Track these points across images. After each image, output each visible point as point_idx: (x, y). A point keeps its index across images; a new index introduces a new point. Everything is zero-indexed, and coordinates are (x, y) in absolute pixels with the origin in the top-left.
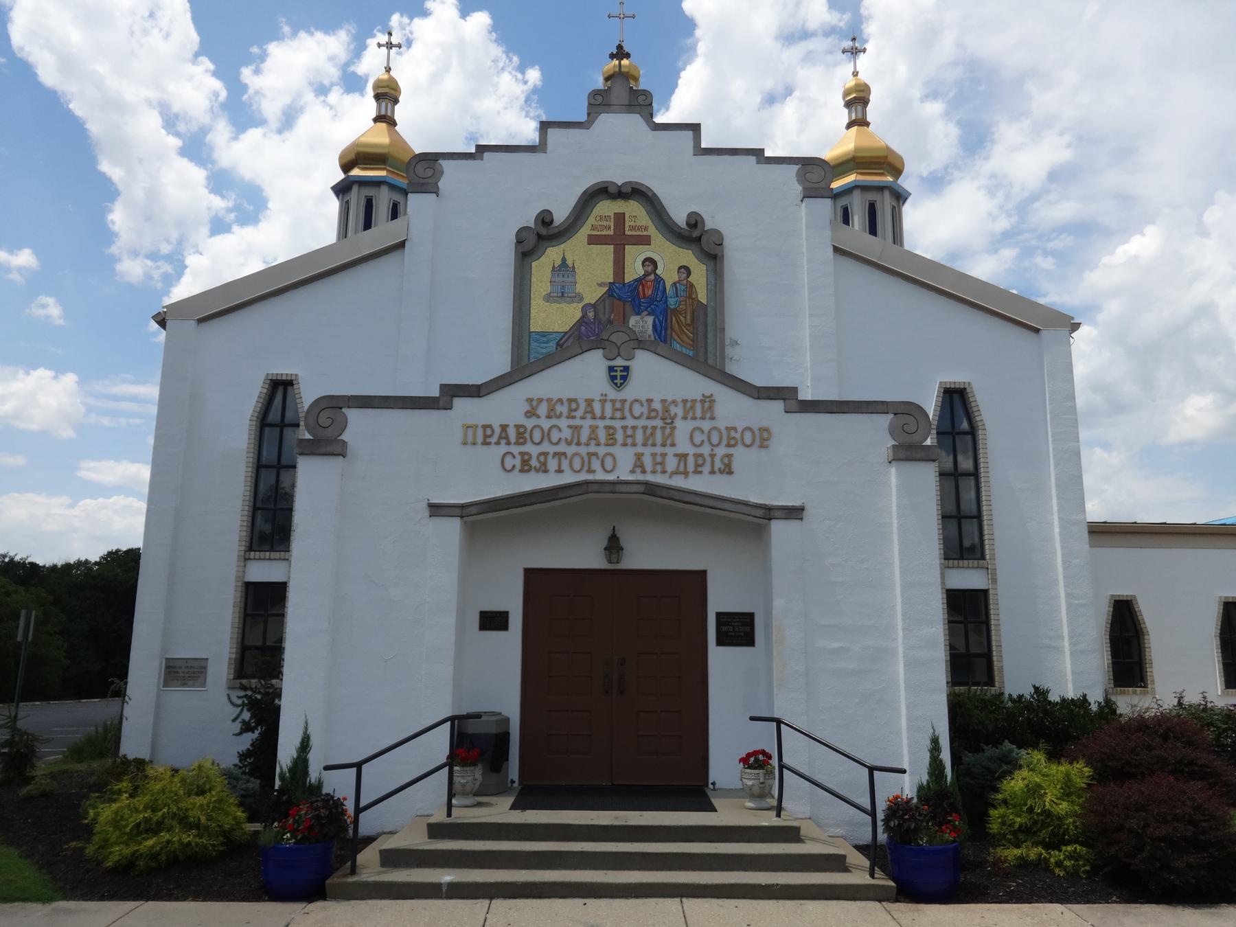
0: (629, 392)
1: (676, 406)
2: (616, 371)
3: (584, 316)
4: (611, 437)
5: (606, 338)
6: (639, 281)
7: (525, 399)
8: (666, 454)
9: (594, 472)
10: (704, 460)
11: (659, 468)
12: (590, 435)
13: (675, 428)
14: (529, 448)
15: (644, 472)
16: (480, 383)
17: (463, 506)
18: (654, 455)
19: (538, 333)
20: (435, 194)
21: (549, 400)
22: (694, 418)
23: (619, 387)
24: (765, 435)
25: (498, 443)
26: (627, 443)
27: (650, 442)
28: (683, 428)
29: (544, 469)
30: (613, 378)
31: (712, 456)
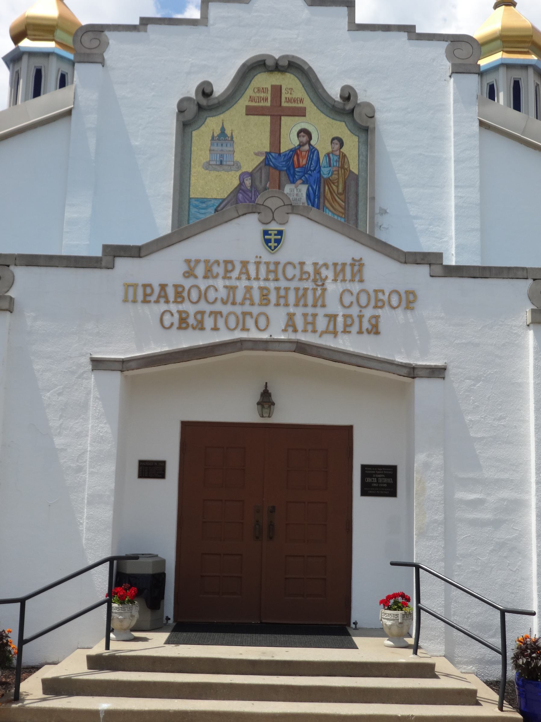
2: (271, 235)
3: (242, 183)
6: (295, 151)
7: (184, 260)
14: (186, 306)
15: (295, 331)
16: (139, 243)
17: (123, 361)
18: (305, 315)
19: (197, 199)
20: (100, 66)
21: (207, 262)
22: (344, 280)
23: (273, 250)
25: (157, 302)
27: (302, 303)
30: (267, 241)
31: (361, 317)
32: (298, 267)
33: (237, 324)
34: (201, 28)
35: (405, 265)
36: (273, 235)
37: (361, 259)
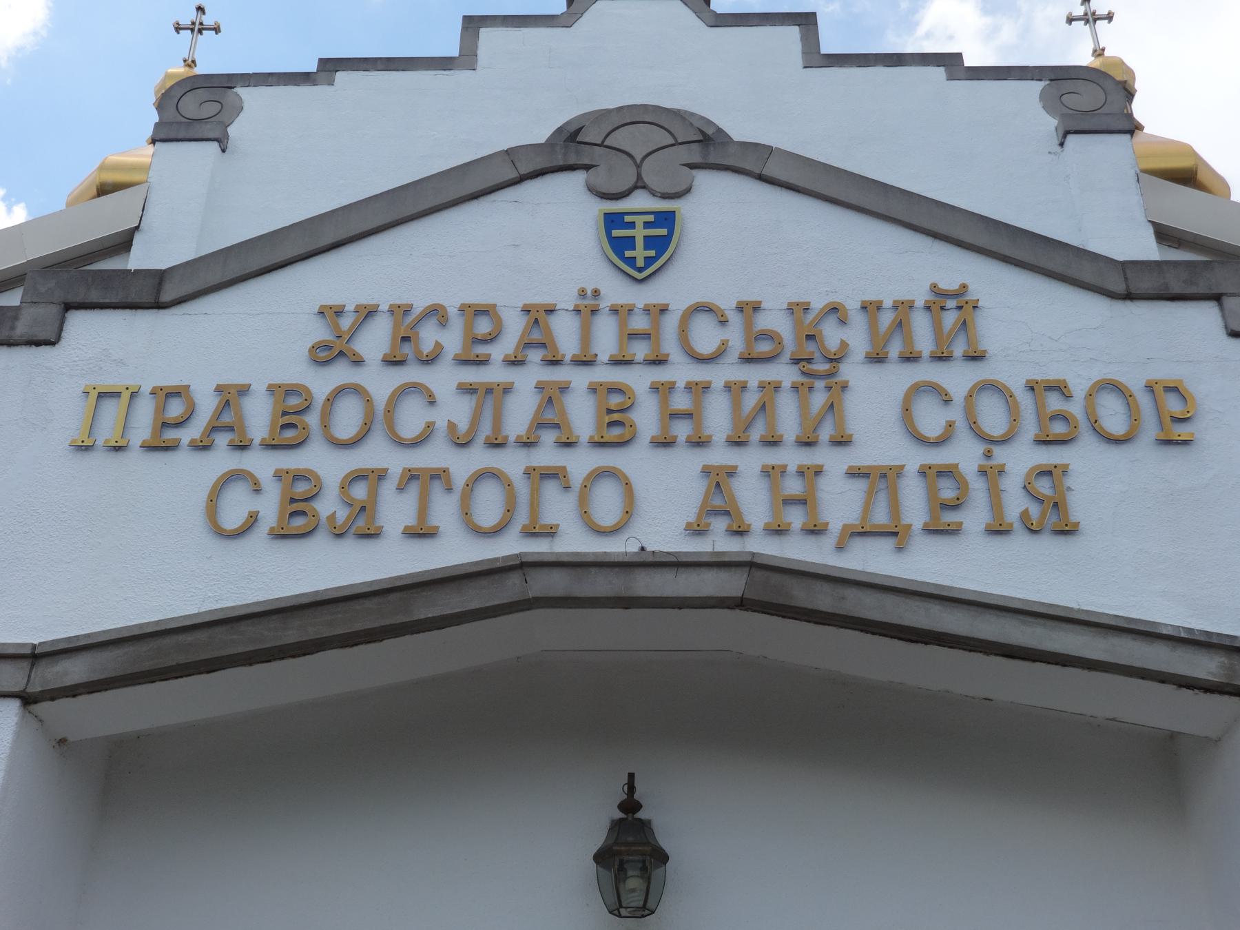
1: (843, 322)
2: (632, 225)
4: (616, 417)
5: (599, 142)
7: (316, 309)
8: (818, 471)
9: (550, 533)
10: (962, 485)
11: (796, 517)
12: (538, 412)
13: (844, 387)
15: (740, 532)
16: (163, 266)
17: (35, 656)
18: (772, 473)
20: (215, 145)
21: (400, 311)
22: (910, 358)
23: (640, 270)
24: (1174, 405)
25: (202, 446)
27: (757, 432)
30: (620, 246)
31: (992, 474)
32: (735, 319)
33: (510, 510)
34: (459, 77)
35: (1128, 303)
36: (639, 225)
37: (964, 286)
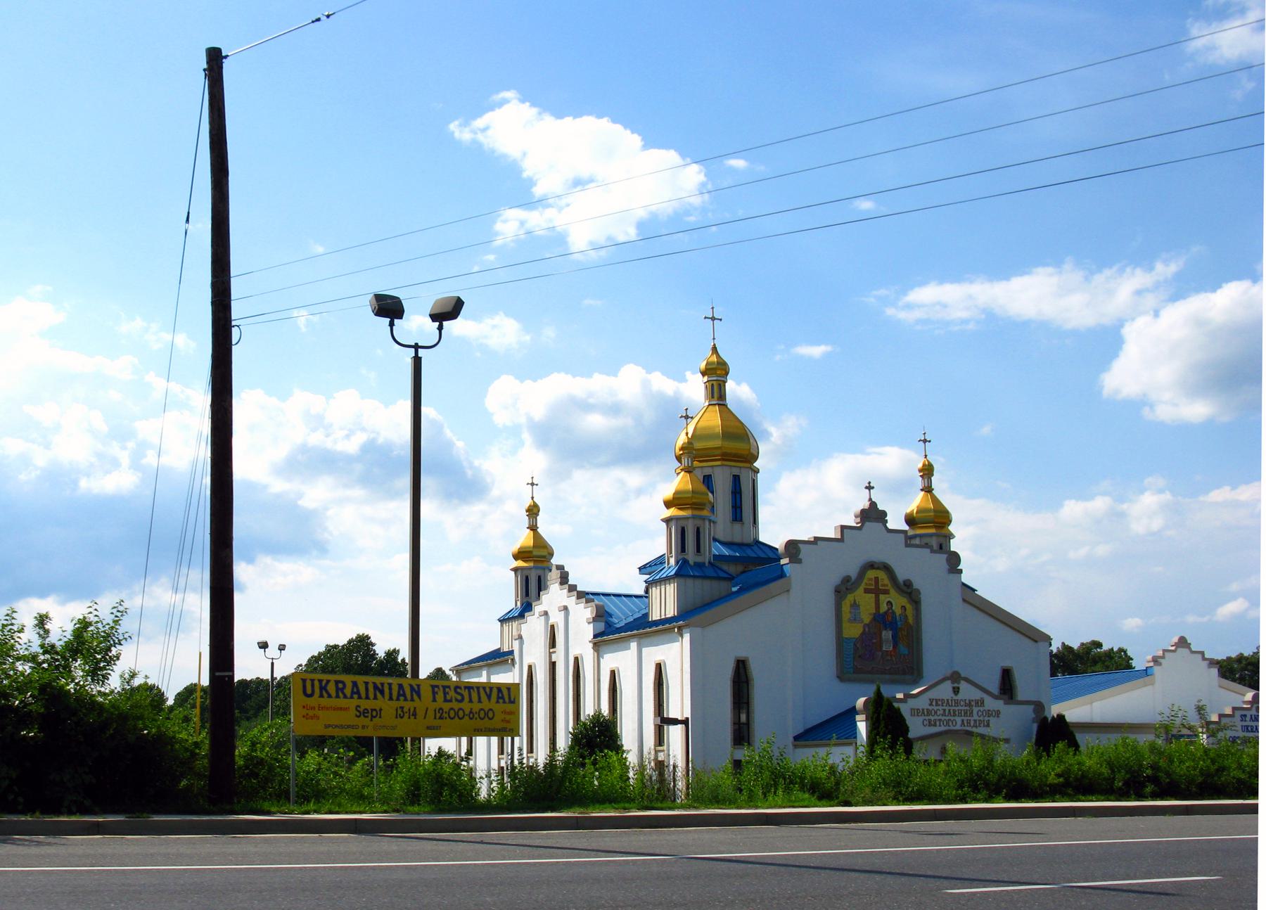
0: (960, 697)
3: (864, 630)
6: (886, 613)
14: (931, 717)
19: (846, 638)
25: (921, 715)
26: (960, 715)
28: (975, 710)
29: (935, 725)
30: (954, 692)
